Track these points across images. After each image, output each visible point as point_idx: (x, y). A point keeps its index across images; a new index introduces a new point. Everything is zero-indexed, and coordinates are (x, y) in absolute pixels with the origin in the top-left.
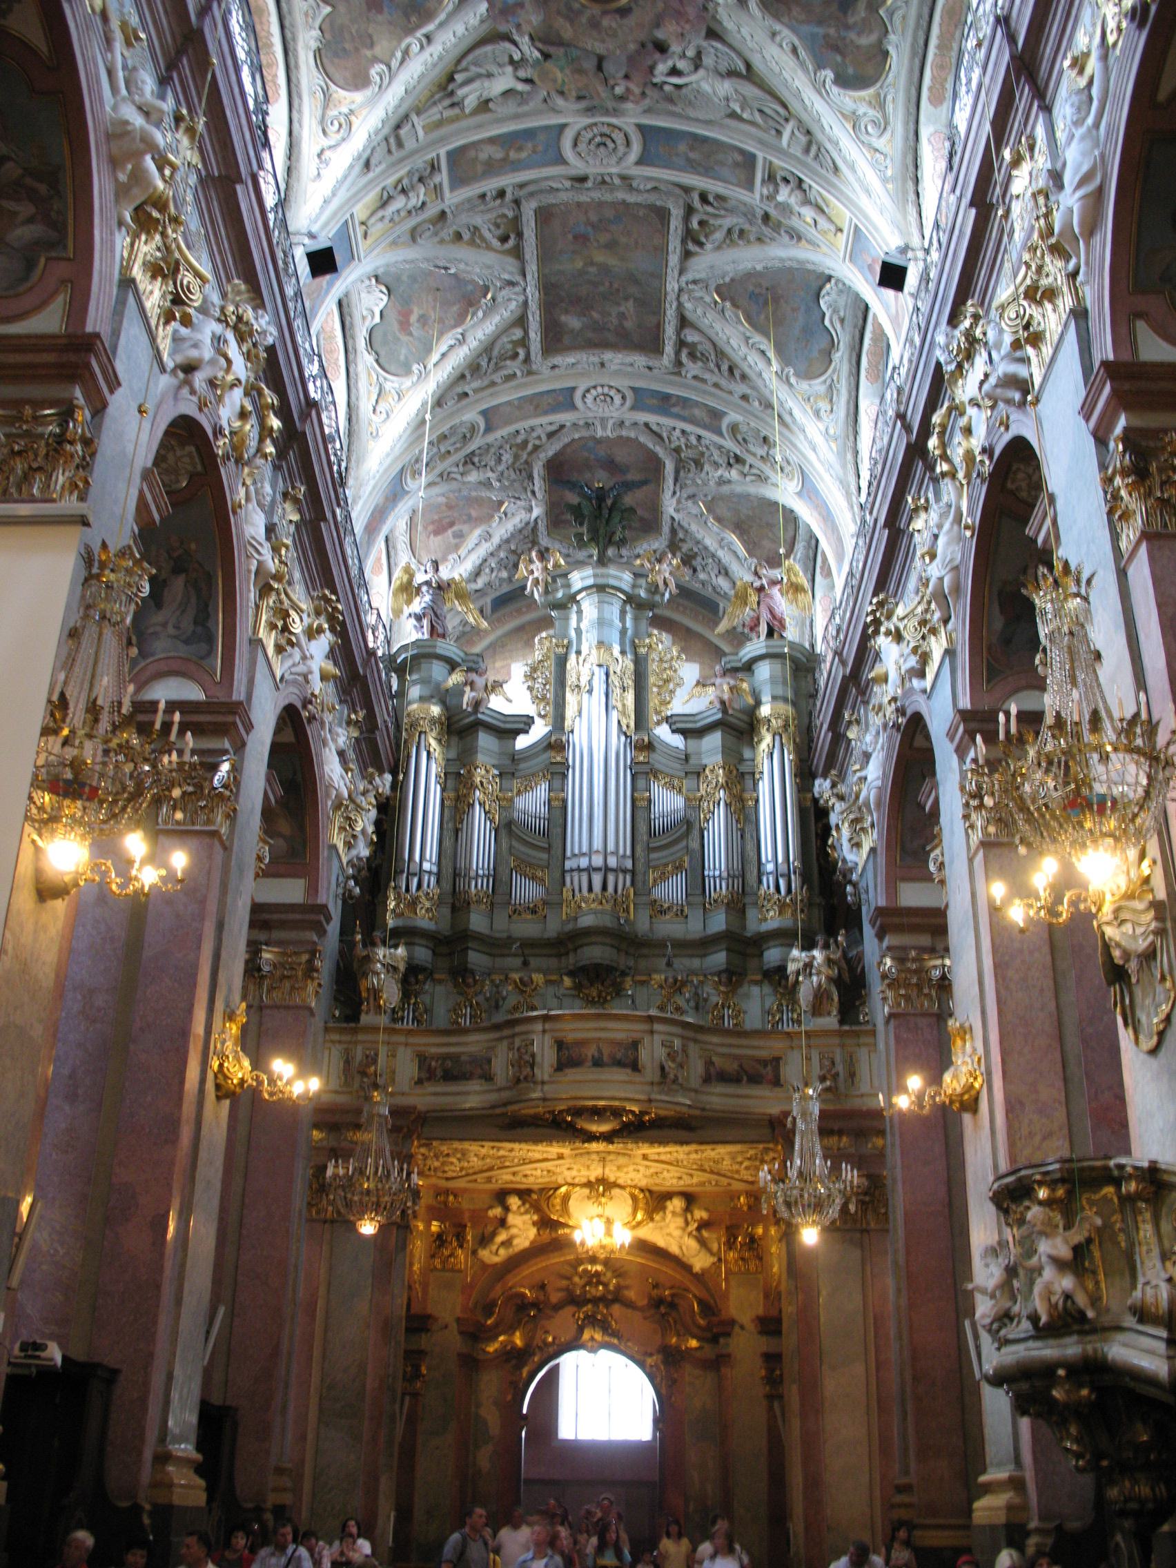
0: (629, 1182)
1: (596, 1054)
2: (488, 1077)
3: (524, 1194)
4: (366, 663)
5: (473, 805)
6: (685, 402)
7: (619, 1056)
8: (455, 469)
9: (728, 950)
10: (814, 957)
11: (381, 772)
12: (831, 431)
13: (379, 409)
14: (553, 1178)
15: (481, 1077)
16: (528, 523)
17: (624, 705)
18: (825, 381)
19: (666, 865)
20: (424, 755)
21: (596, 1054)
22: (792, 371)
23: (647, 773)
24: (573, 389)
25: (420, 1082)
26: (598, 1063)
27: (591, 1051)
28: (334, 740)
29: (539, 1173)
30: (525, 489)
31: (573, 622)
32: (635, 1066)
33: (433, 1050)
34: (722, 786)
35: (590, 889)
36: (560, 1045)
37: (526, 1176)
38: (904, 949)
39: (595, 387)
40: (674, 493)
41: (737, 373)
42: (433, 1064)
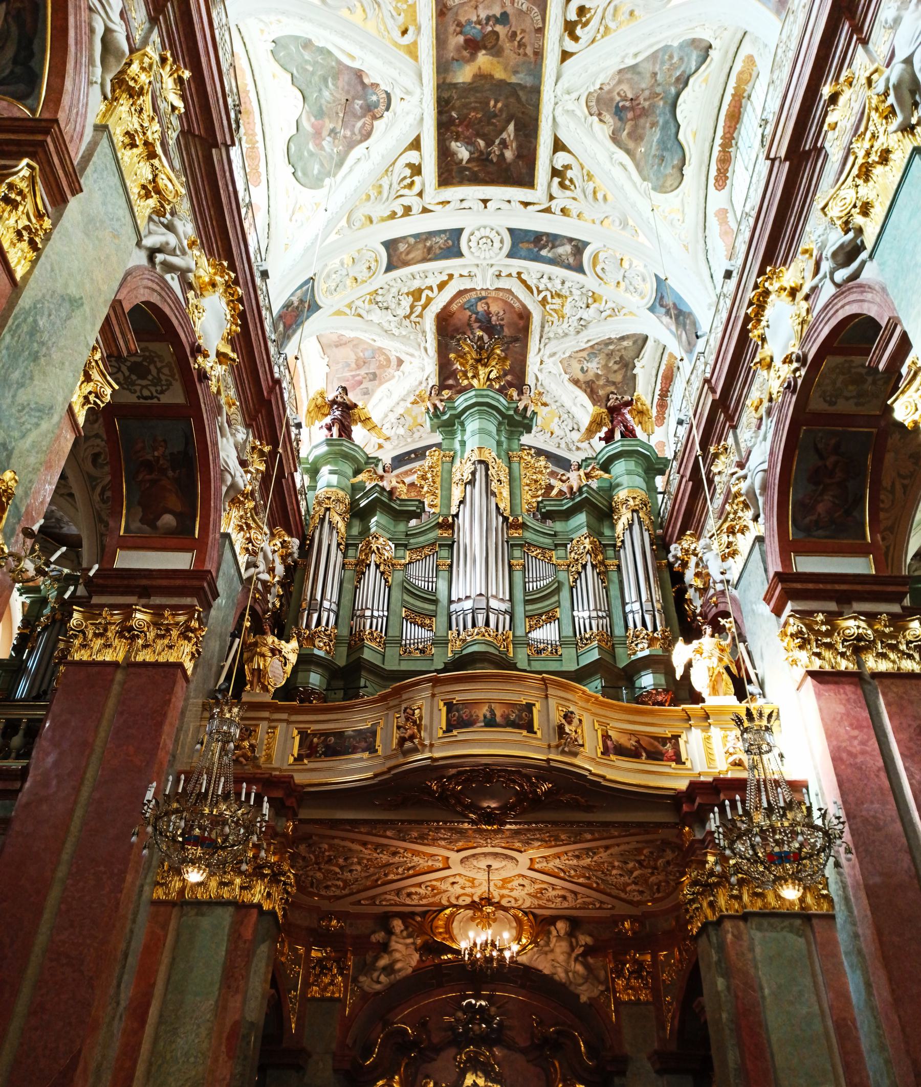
1: (488, 714)
2: (372, 749)
3: (406, 917)
5: (369, 565)
6: (553, 240)
7: (512, 717)
8: (361, 304)
11: (291, 535)
13: (294, 218)
16: (421, 383)
18: (677, 196)
19: (541, 614)
22: (650, 185)
23: (521, 546)
24: (460, 231)
25: (299, 759)
26: (490, 723)
27: (484, 710)
30: (420, 346)
34: (588, 552)
36: (450, 706)
38: (811, 613)
39: (479, 229)
40: (540, 350)
41: (600, 196)
42: (315, 740)
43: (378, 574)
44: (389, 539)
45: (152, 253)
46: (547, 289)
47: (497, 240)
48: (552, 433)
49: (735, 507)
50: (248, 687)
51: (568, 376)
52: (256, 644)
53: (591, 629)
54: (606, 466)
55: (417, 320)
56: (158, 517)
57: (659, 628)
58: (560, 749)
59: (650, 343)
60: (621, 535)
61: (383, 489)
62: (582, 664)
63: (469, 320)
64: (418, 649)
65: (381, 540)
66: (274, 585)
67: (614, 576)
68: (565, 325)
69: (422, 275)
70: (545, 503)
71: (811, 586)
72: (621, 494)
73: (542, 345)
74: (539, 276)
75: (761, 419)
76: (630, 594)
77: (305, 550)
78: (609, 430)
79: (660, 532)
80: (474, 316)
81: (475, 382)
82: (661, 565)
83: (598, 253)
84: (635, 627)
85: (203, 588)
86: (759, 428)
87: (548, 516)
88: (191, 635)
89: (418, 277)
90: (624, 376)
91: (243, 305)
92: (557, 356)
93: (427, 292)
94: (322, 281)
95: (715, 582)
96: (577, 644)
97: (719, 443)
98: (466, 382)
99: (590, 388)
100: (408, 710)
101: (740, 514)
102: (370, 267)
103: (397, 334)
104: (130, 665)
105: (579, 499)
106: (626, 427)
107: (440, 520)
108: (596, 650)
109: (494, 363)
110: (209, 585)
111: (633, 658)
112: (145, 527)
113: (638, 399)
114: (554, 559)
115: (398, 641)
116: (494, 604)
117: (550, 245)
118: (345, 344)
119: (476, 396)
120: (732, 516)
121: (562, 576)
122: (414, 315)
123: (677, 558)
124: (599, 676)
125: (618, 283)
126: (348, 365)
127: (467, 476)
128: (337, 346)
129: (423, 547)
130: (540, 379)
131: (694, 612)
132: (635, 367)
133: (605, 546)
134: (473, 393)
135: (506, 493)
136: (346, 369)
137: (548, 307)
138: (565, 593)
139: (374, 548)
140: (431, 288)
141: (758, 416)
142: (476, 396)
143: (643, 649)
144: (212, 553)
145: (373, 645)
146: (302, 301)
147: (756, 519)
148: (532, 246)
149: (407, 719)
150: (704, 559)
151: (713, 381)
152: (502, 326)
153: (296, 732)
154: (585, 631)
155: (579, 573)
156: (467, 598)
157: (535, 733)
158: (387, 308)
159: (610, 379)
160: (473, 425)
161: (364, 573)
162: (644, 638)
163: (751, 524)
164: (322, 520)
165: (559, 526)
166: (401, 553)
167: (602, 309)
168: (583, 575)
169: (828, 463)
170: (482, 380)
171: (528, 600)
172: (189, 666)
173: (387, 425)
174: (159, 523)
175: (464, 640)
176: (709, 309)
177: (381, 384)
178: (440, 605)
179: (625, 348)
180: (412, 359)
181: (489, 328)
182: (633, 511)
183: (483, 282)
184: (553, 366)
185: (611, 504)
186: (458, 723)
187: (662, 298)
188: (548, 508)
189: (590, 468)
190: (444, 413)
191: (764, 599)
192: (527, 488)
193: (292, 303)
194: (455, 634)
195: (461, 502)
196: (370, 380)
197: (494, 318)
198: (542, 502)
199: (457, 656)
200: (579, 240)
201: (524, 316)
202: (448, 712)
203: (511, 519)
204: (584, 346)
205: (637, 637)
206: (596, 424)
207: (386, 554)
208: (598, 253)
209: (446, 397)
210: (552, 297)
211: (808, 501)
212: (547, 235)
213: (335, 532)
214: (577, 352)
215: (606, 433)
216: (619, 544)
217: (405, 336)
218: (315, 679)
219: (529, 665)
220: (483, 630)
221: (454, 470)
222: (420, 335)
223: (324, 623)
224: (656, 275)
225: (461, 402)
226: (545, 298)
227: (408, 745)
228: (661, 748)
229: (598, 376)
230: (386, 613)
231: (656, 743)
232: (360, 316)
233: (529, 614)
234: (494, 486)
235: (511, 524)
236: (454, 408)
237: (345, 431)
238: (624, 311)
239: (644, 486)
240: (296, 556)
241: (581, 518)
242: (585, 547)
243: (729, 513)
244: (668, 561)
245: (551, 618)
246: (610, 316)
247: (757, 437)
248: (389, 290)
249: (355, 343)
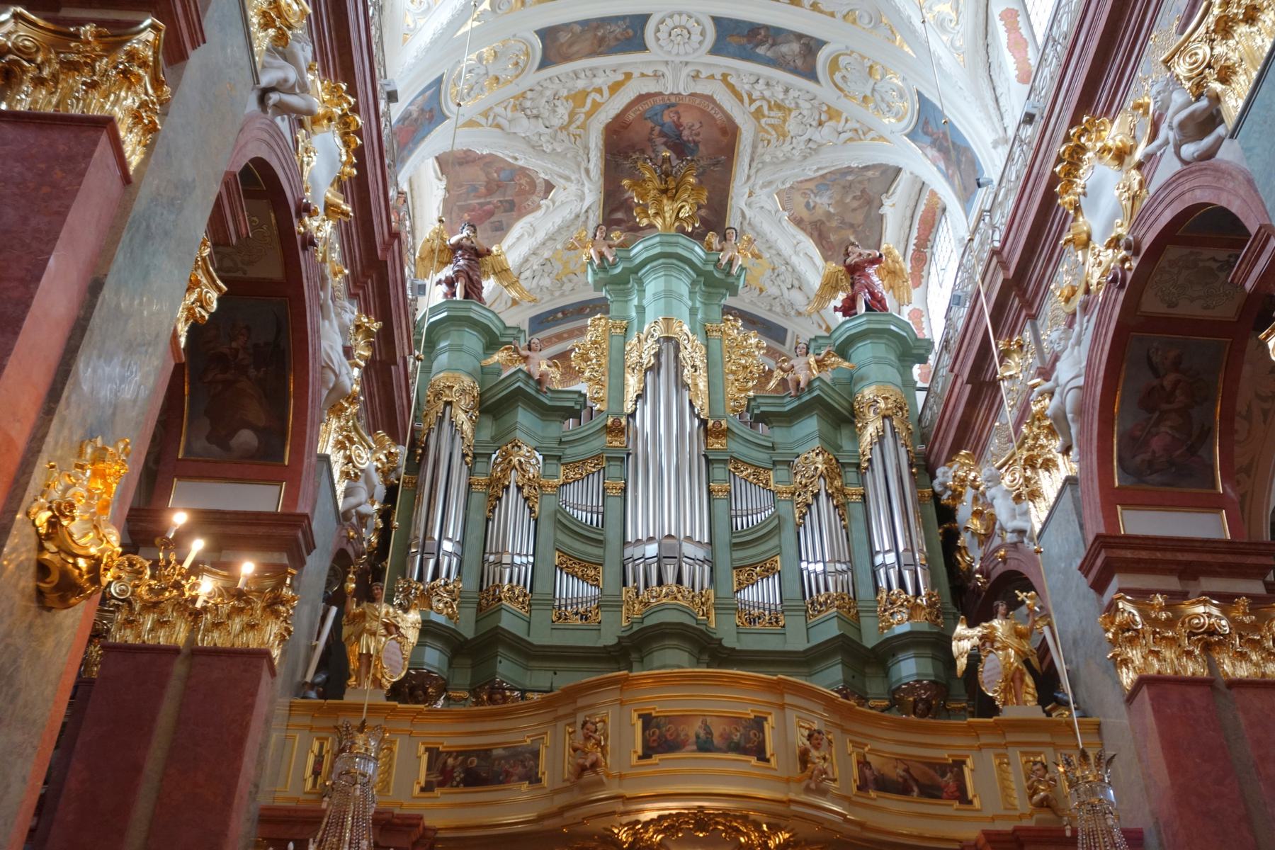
1: (702, 734)
2: (534, 779)
4: (387, 247)
5: (507, 487)
6: (773, 35)
7: (737, 737)
9: (843, 663)
10: (994, 628)
11: (396, 439)
12: (958, 44)
15: (522, 779)
16: (578, 216)
17: (696, 385)
20: (446, 424)
21: (702, 734)
23: (725, 462)
25: (427, 788)
26: (705, 745)
27: (695, 728)
28: (338, 315)
30: (579, 166)
31: (635, 302)
32: (760, 753)
34: (821, 475)
35: (660, 582)
36: (647, 720)
39: (671, 16)
40: (749, 177)
42: (450, 761)
43: (521, 501)
44: (535, 449)
45: (264, 94)
46: (763, 98)
47: (696, 30)
48: (761, 291)
49: (1035, 430)
50: (352, 682)
51: (787, 213)
52: (363, 616)
53: (827, 589)
54: (843, 351)
55: (578, 131)
56: (233, 433)
57: (923, 593)
58: (804, 784)
59: (904, 178)
60: (868, 452)
61: (529, 375)
62: (814, 643)
63: (651, 134)
64: (577, 613)
65: (525, 448)
66: (371, 516)
67: (857, 510)
68: (787, 147)
69: (589, 73)
70: (759, 400)
71: (1144, 555)
72: (868, 393)
73: (753, 171)
74: (753, 79)
75: (1074, 314)
76: (882, 540)
77: (416, 461)
78: (848, 298)
79: (921, 447)
80: (658, 128)
81: (658, 222)
82: (923, 496)
83: (837, 57)
84: (890, 588)
85: (296, 540)
86: (1070, 325)
87: (764, 418)
88: (282, 608)
89: (583, 75)
90: (867, 216)
91: (362, 139)
92: (774, 187)
93: (593, 95)
94: (451, 82)
95: (1002, 529)
96: (807, 611)
97: (1011, 336)
98: (645, 222)
99: (819, 232)
100: (589, 725)
101: (1043, 441)
102: (517, 64)
103: (548, 151)
104: (196, 653)
105: (807, 398)
106: (872, 294)
107: (610, 421)
108: (835, 622)
109: (685, 196)
110: (304, 534)
111: (887, 634)
112: (214, 448)
113: (889, 253)
114: (772, 482)
115: (550, 601)
116: (688, 549)
117: (770, 41)
118: (474, 161)
119: (661, 243)
120: (1030, 442)
121: (784, 508)
122: (574, 126)
123: (946, 488)
124: (839, 658)
125: (865, 97)
126: (475, 189)
127: (648, 359)
128: (461, 164)
129: (584, 462)
130: (748, 217)
131: (970, 566)
132: (882, 205)
133: (843, 464)
134: (658, 239)
135: (702, 385)
136: (472, 194)
137: (763, 121)
138: (788, 534)
139: (515, 461)
140: (599, 91)
141: (1069, 309)
142: (661, 243)
143: (900, 622)
144: (306, 486)
145: (515, 607)
146: (422, 111)
147: (1066, 451)
148: (744, 41)
149: (587, 738)
150: (988, 494)
151: (1005, 253)
152: (696, 143)
154: (818, 591)
155: (809, 506)
156: (650, 540)
157: (768, 761)
158: (537, 117)
159: (846, 220)
160: (653, 286)
161: (499, 499)
162: (902, 605)
163: (1060, 459)
164: (441, 419)
165: (778, 435)
166: (552, 469)
167: (840, 130)
168: (814, 508)
169: (1165, 383)
170: (668, 219)
171: (736, 545)
172: (276, 653)
173: (528, 274)
174: (234, 442)
175: (647, 604)
176: (995, 147)
177: (521, 216)
178: (608, 547)
179: (869, 180)
180: (567, 184)
181: (680, 147)
182: (884, 417)
183: (676, 84)
184: (768, 200)
185: (852, 405)
186: (659, 745)
187: (926, 123)
188: (763, 409)
189: (823, 353)
190: (614, 265)
191: (1080, 568)
192: (731, 377)
193: (410, 115)
194: (632, 594)
195: (639, 397)
196: (506, 211)
197: (686, 133)
198: (755, 398)
199: (636, 628)
200: (812, 38)
201: (730, 132)
202: (645, 728)
203: (711, 423)
204: (811, 174)
205: (893, 603)
206: (830, 286)
207: (532, 470)
208: (837, 57)
209: (617, 242)
210: (770, 108)
211: (1138, 433)
212: (767, 28)
213: (458, 437)
214: (801, 182)
215: (843, 301)
216: (866, 465)
217: (558, 154)
218: (433, 658)
219: (738, 640)
220: (675, 589)
221: (628, 348)
222: (581, 152)
223: (444, 574)
224: (919, 93)
225: (639, 251)
226: (759, 109)
227: (588, 776)
228: (940, 780)
229: (829, 215)
230: (531, 559)
231: (932, 772)
232: (498, 126)
233: (737, 564)
234: (687, 372)
235: (708, 430)
236: (629, 259)
237: (473, 291)
238: (871, 135)
239: (898, 380)
240: (402, 470)
241: (811, 425)
242: (816, 468)
243: (1026, 438)
244: (933, 491)
245: (769, 572)
246: (851, 139)
247: (1068, 339)
248: (541, 93)
249: (488, 162)
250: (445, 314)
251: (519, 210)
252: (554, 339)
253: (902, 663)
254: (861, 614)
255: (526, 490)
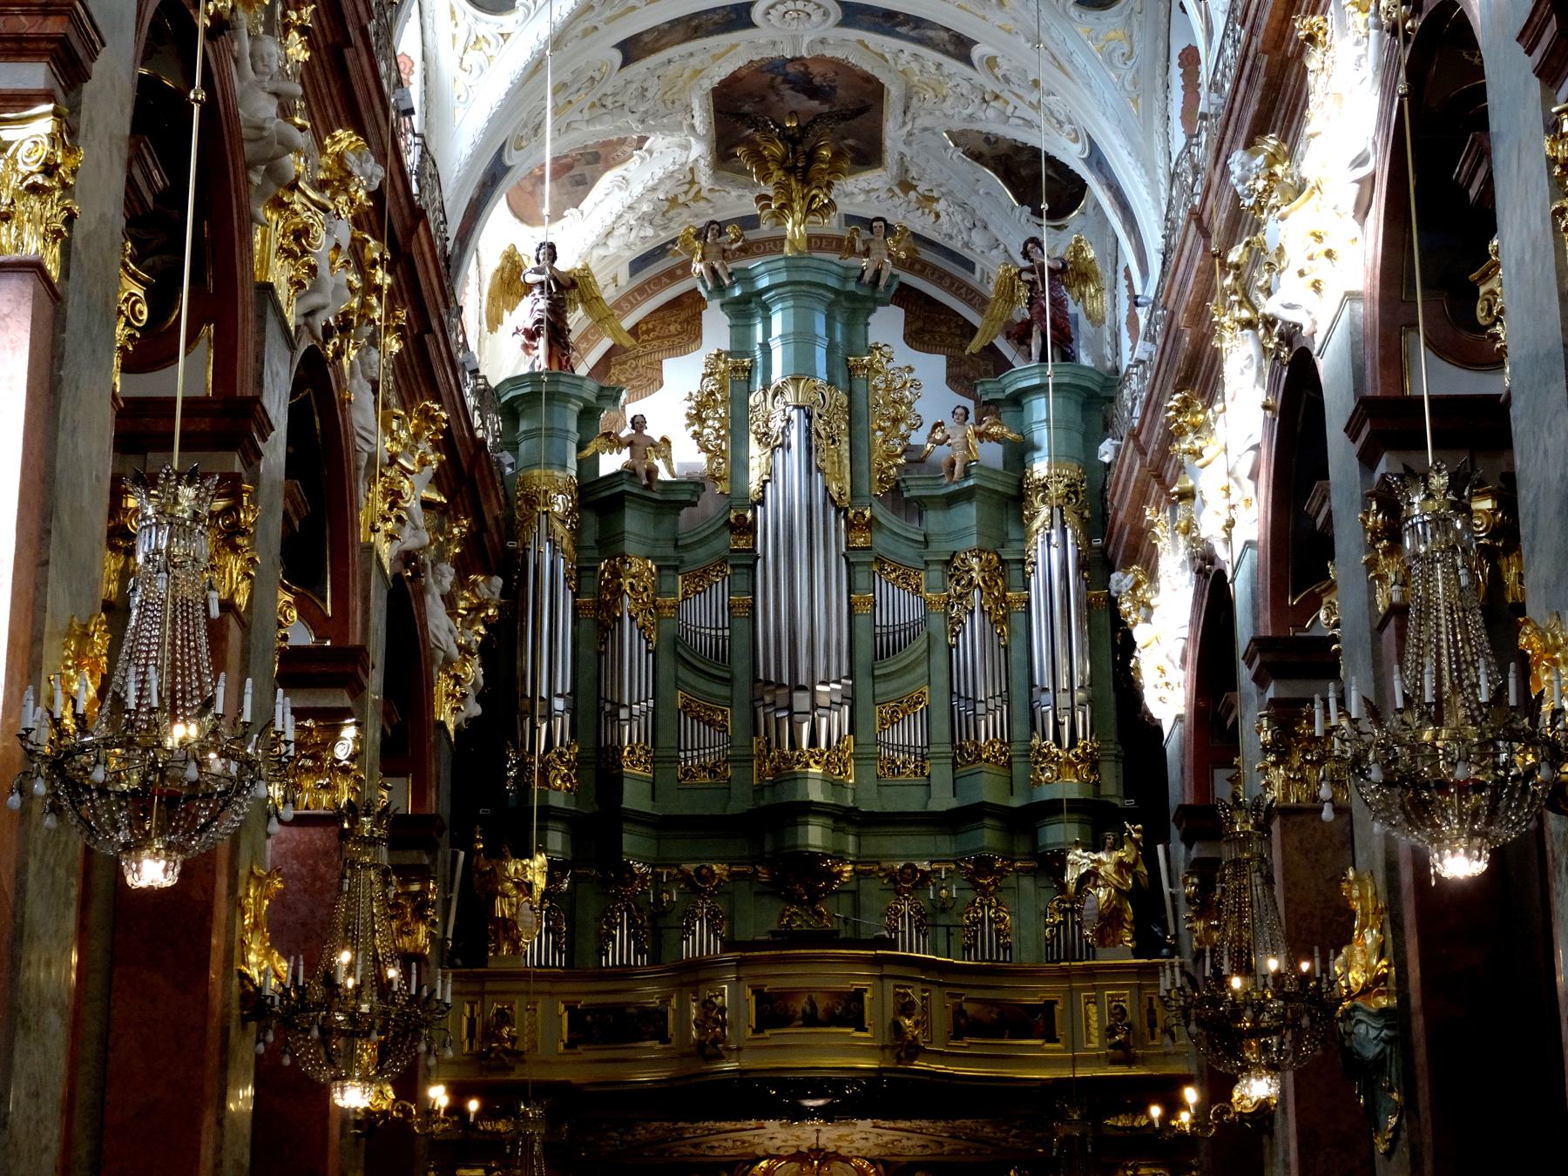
0: (855, 1153)
1: (808, 1009)
6: (918, 22)
8: (579, 117)
11: (488, 573)
14: (749, 1150)
23: (869, 564)
26: (811, 1020)
27: (801, 1005)
28: (438, 583)
29: (730, 1144)
31: (759, 329)
33: (584, 1001)
37: (712, 1148)
58: (896, 1051)
79: (1098, 542)
80: (779, 79)
107: (732, 516)
114: (922, 588)
134: (782, 263)
138: (939, 659)
145: (638, 770)
153: (562, 1007)
162: (1052, 760)
177: (608, 167)
196: (588, 163)
250: (528, 390)
251: (607, 161)
252: (665, 280)
253: (1049, 828)
254: (1014, 759)
255: (640, 620)
